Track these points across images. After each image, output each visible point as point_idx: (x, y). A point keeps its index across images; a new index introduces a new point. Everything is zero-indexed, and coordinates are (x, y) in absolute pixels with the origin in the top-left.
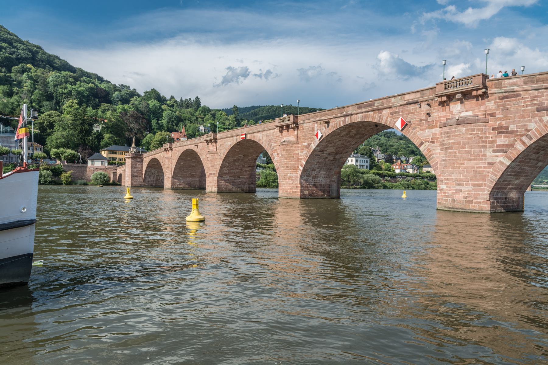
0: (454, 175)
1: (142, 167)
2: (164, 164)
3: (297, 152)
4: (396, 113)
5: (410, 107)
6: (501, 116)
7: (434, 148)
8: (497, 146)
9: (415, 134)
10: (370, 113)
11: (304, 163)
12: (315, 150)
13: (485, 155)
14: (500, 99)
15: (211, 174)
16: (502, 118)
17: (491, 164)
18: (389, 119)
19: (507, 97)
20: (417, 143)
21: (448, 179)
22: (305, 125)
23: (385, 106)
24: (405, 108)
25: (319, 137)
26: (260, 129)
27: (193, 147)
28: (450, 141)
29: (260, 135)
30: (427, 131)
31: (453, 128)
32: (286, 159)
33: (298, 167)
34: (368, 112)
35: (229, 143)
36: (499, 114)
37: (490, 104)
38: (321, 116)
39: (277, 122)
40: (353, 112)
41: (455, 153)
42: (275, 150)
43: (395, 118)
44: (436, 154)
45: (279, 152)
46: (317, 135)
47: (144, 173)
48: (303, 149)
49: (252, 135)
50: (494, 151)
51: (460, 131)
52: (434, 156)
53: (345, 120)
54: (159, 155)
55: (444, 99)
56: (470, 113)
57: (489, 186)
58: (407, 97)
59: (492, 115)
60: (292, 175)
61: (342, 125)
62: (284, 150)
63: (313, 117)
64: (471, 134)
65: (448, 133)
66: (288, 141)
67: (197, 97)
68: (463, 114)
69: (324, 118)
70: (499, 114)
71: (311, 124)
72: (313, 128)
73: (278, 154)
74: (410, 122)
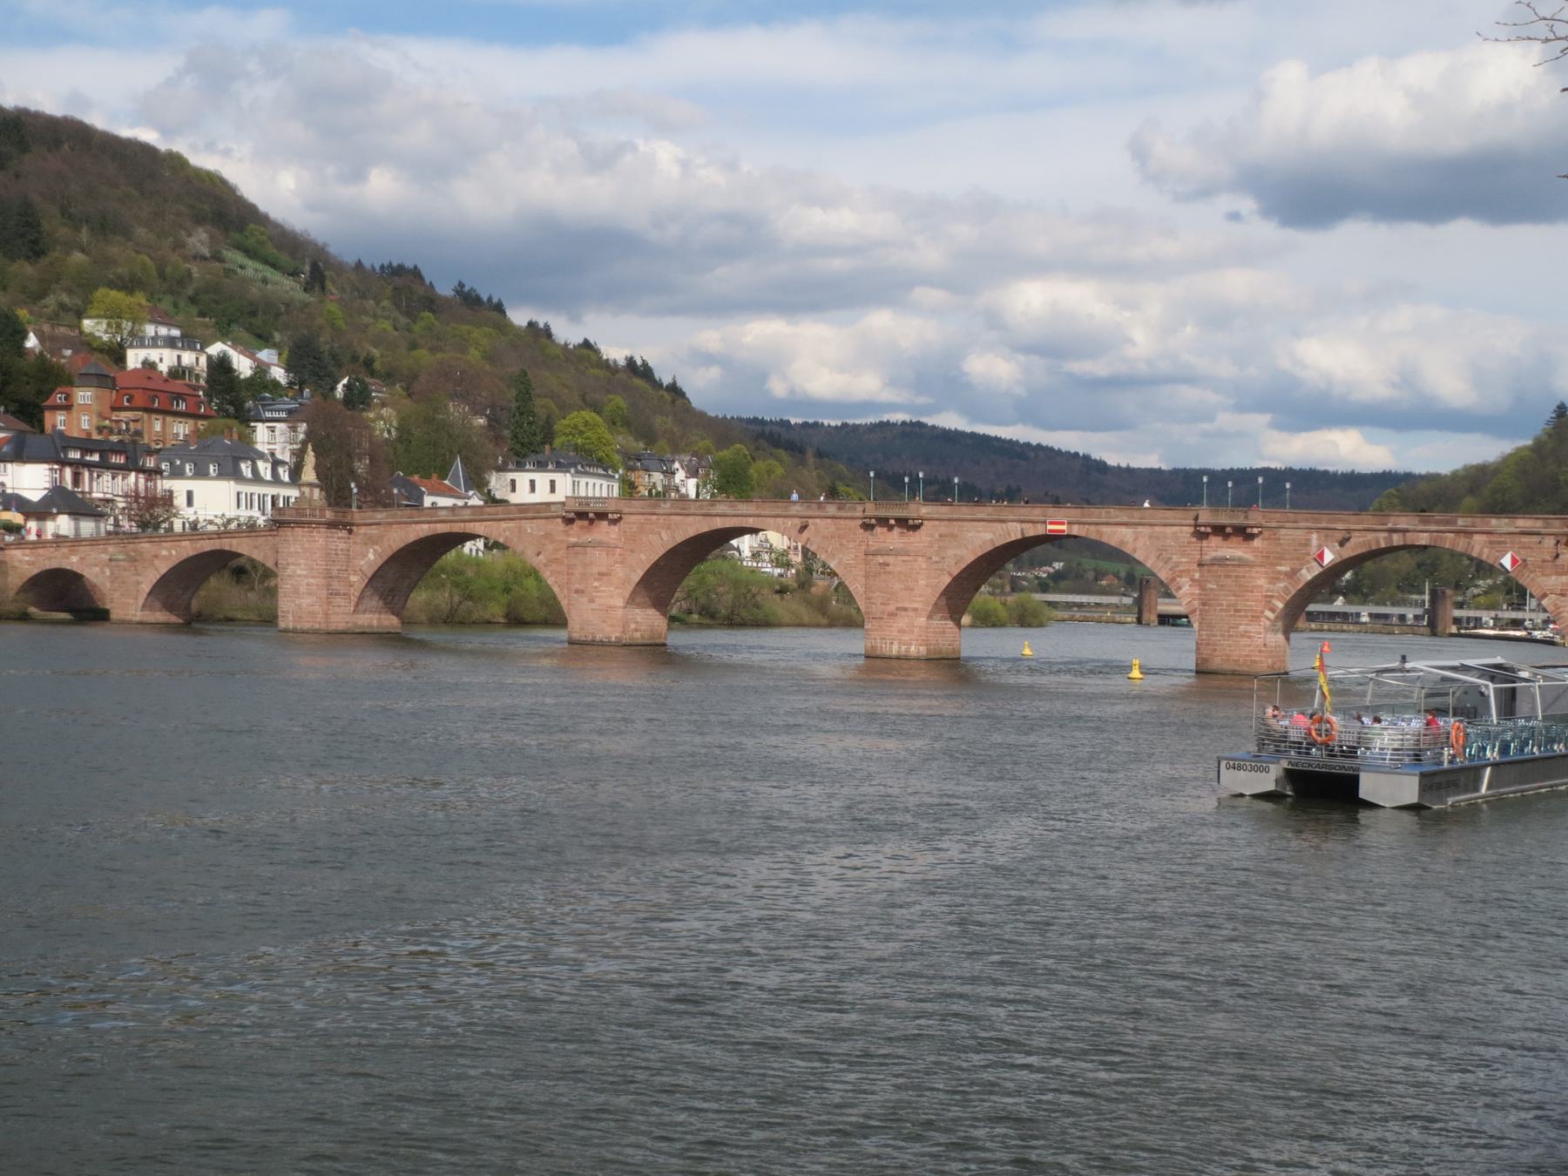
5: (1525, 539)
11: (1280, 605)
15: (905, 609)
22: (1283, 531)
24: (1517, 538)
26: (1125, 519)
35: (988, 536)
38: (1329, 521)
45: (1197, 576)
46: (1321, 556)
49: (1093, 528)
53: (1390, 539)
54: (504, 525)
60: (1249, 628)
63: (1307, 520)
66: (1240, 559)
69: (1340, 526)
71: (1299, 532)
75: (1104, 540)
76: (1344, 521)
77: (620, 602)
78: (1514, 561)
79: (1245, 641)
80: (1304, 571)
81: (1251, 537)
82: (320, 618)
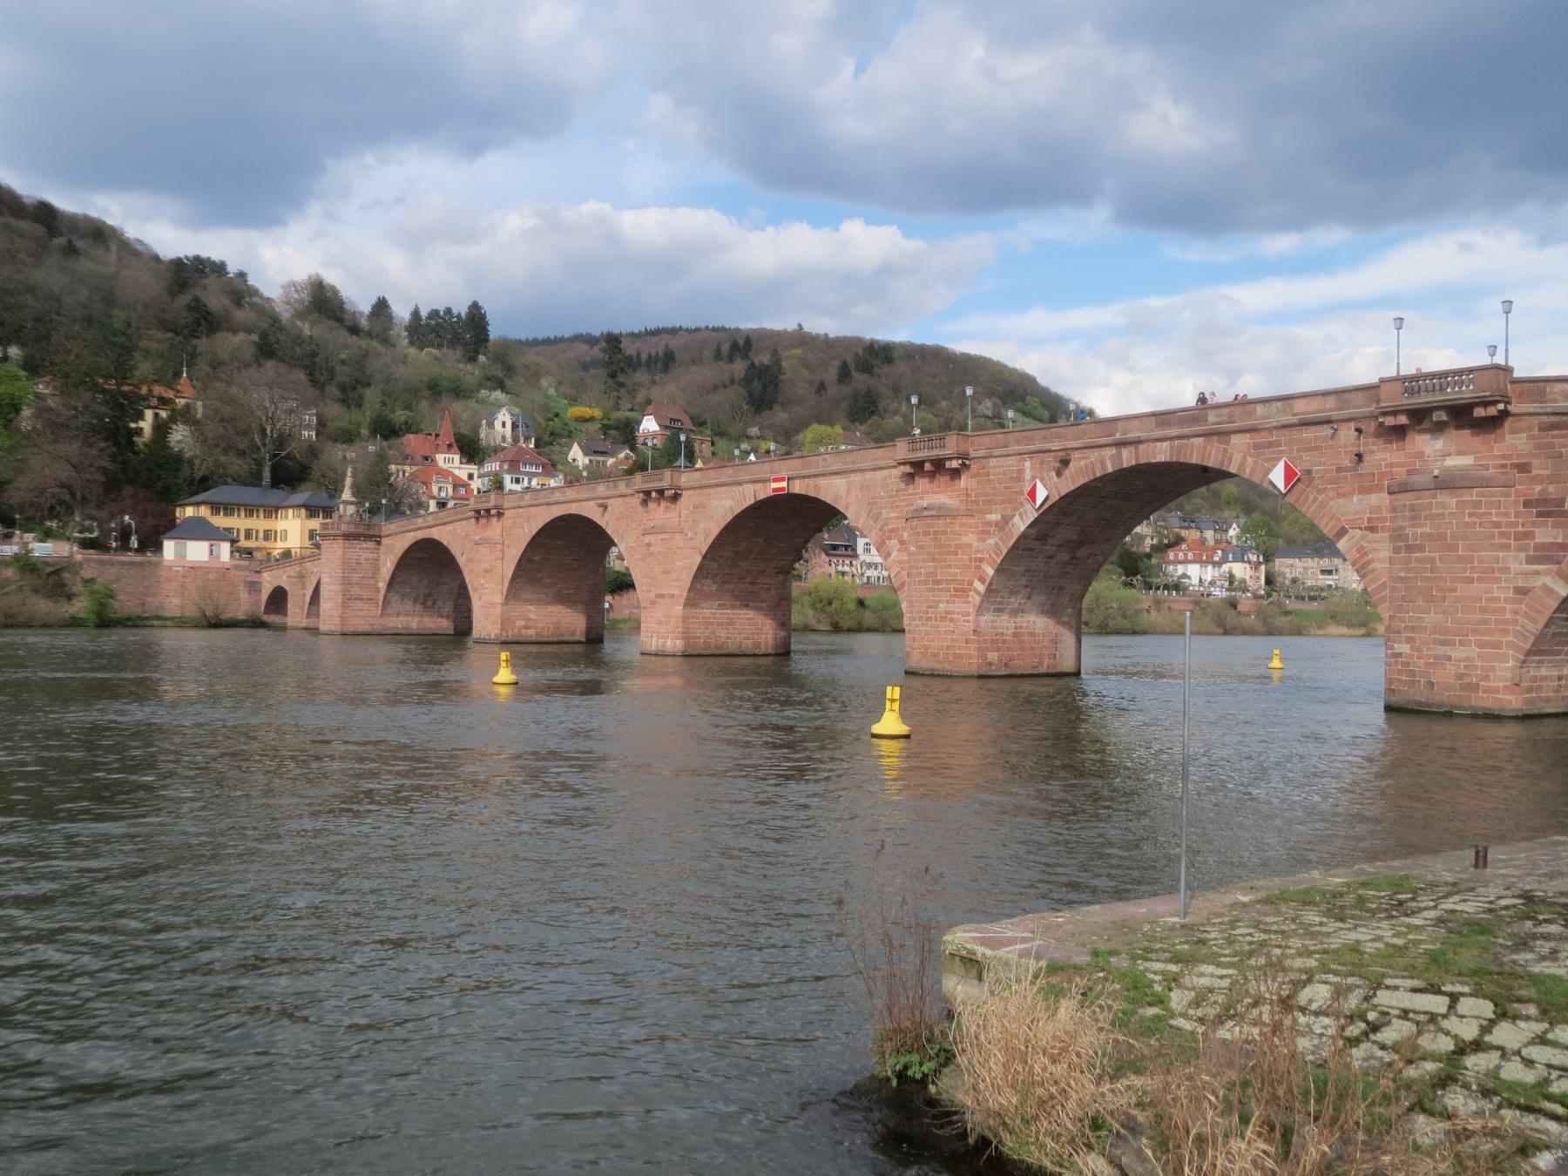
0: (1431, 618)
1: (377, 568)
2: (470, 560)
3: (966, 540)
4: (1270, 445)
5: (1308, 434)
6: (1545, 472)
7: (1375, 545)
8: (1538, 547)
9: (1322, 505)
10: (1193, 440)
11: (990, 572)
12: (1023, 536)
13: (1506, 570)
14: (1541, 430)
15: (662, 596)
16: (1548, 477)
17: (1522, 592)
18: (1250, 460)
19: (1556, 426)
20: (1328, 529)
21: (1413, 629)
22: (993, 462)
23: (1239, 424)
25: (1039, 501)
26: (838, 467)
27: (589, 510)
28: (1420, 531)
29: (840, 482)
30: (1355, 499)
31: (1425, 498)
32: (934, 560)
33: (971, 583)
34: (1189, 437)
35: (728, 503)
36: (1540, 469)
37: (1516, 441)
38: (1045, 439)
39: (902, 450)
40: (1143, 435)
41: (1432, 560)
42: (891, 531)
43: (1269, 460)
44: (1381, 561)
46: (1032, 494)
47: (382, 585)
48: (988, 533)
49: (811, 481)
50: (1530, 561)
51: (1444, 505)
52: (1376, 565)
53: (1119, 455)
54: (449, 528)
55: (1403, 420)
56: (1467, 461)
57: (1516, 648)
58: (1300, 406)
59: (1523, 468)
60: (952, 607)
61: (1110, 470)
62: (926, 533)
63: (1018, 442)
64: (1470, 515)
65: (1412, 508)
66: (940, 507)
67: (475, 306)
68: (1450, 462)
69: (1055, 446)
70: (1540, 469)
71: (1011, 461)
72: (1021, 471)
73: (902, 543)
74: (1309, 472)
75: (821, 497)
76: (1059, 437)
77: (499, 599)
78: (1289, 474)
79: (945, 626)
80: (1017, 519)
81: (956, 473)
82: (336, 620)
